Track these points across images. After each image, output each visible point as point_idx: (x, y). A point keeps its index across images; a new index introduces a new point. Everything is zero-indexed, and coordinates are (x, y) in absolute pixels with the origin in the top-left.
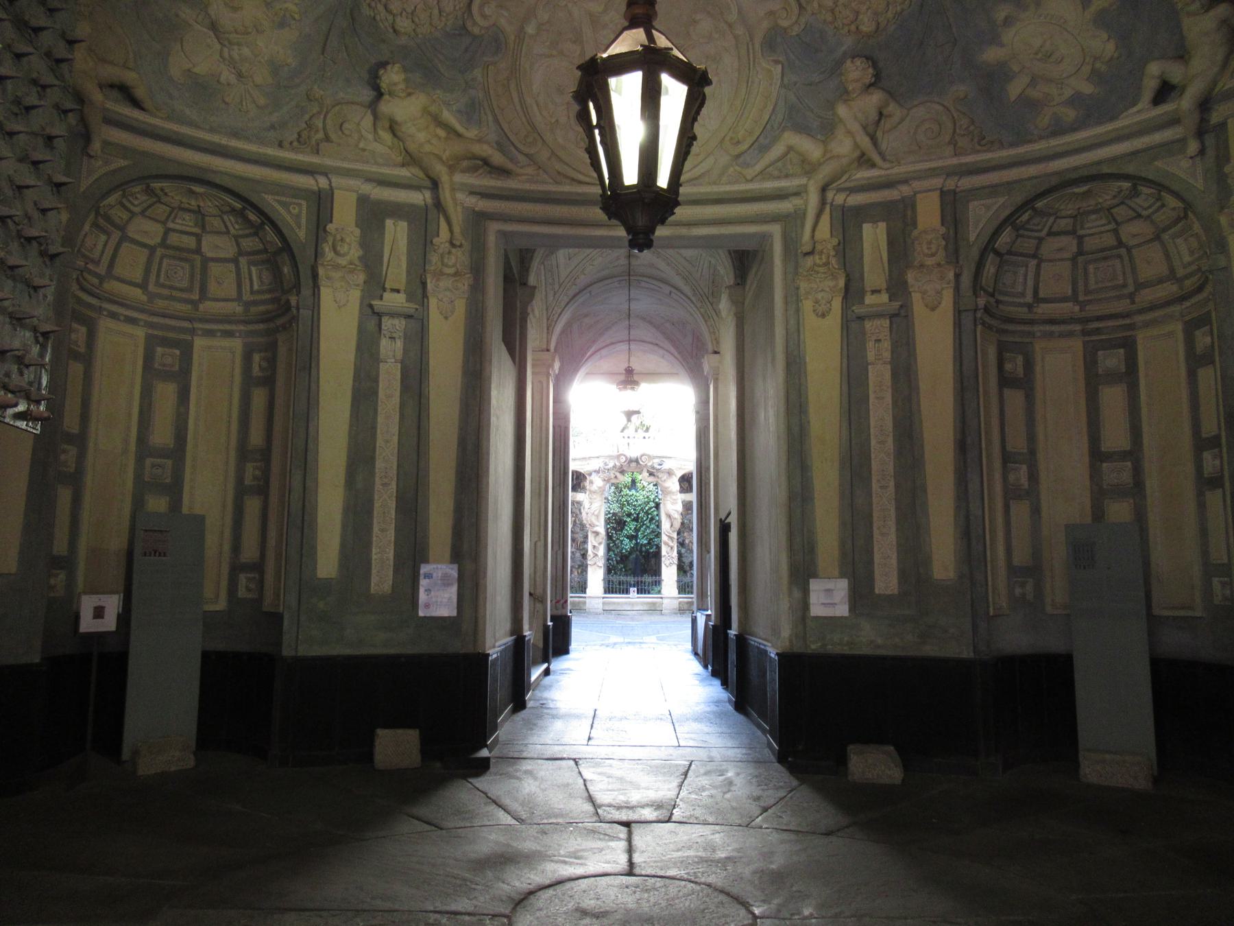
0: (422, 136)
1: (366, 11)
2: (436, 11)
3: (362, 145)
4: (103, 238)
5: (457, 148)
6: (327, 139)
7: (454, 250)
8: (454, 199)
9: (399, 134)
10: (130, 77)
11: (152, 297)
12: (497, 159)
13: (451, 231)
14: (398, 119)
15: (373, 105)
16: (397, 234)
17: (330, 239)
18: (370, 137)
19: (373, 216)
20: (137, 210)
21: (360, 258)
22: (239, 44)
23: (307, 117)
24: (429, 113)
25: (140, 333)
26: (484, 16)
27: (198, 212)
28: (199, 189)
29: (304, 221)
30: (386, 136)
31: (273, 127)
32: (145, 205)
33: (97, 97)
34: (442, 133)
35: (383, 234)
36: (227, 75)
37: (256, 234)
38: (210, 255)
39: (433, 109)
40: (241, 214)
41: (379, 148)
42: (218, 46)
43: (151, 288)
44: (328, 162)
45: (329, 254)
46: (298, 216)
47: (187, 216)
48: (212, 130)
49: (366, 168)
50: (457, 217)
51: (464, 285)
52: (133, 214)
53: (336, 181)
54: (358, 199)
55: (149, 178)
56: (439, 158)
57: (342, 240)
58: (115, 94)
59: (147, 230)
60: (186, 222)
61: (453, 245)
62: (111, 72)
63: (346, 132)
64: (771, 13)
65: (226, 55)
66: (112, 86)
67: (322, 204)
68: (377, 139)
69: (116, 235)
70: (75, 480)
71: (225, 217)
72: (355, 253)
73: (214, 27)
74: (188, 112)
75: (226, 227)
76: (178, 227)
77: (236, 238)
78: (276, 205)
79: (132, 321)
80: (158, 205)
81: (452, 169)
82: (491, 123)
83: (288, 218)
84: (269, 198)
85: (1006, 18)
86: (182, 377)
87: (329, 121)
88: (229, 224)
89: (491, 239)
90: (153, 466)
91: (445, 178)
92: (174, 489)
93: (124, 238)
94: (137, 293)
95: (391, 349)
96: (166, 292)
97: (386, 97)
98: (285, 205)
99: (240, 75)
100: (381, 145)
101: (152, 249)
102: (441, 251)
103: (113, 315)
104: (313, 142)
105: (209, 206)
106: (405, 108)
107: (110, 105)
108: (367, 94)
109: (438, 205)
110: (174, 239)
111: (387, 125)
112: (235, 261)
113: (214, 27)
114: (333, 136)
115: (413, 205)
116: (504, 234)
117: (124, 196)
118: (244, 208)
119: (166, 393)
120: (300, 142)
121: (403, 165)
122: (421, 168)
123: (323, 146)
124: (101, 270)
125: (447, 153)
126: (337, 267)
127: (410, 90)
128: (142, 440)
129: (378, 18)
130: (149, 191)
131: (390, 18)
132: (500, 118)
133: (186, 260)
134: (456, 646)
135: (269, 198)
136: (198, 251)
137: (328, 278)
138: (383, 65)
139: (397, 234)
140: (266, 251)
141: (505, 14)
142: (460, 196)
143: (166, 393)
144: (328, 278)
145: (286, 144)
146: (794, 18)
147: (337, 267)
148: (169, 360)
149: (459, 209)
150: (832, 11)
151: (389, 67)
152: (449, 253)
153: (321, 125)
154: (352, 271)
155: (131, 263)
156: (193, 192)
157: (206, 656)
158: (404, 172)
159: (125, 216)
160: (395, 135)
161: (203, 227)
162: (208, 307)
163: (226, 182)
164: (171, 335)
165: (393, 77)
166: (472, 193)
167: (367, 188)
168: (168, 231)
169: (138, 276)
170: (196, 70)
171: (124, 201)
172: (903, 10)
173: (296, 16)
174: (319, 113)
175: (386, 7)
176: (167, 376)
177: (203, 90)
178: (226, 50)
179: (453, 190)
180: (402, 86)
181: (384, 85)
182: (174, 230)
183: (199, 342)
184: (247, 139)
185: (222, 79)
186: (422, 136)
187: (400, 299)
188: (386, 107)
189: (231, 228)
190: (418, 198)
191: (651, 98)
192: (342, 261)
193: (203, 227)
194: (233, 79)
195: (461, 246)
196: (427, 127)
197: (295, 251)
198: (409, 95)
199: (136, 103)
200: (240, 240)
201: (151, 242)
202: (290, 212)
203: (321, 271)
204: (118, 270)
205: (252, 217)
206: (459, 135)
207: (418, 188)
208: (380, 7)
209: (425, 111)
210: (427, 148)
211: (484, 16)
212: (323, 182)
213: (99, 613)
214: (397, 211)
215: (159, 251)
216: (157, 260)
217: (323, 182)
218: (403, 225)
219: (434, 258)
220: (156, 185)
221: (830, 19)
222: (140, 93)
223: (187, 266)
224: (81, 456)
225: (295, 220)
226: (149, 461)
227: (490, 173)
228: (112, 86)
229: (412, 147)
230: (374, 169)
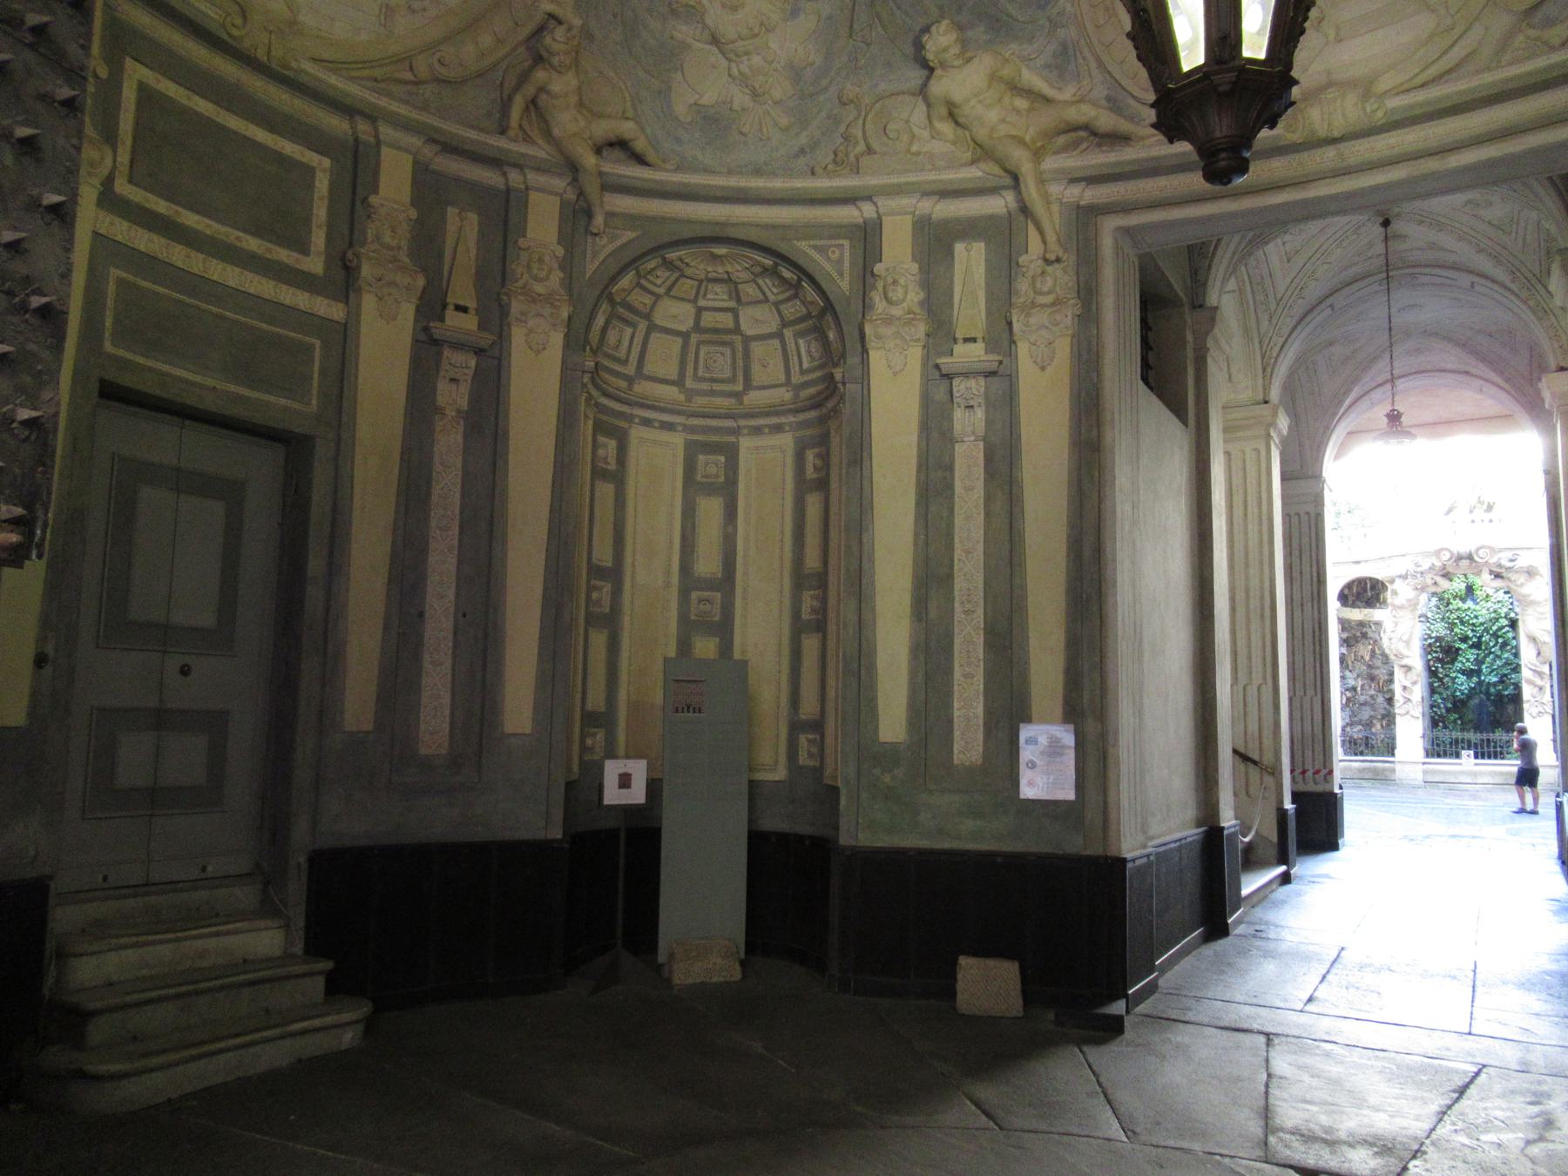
0: (993, 116)
3: (914, 149)
4: (629, 331)
5: (1046, 119)
6: (870, 151)
7: (1049, 269)
8: (1047, 199)
9: (962, 120)
10: (627, 129)
11: (691, 394)
12: (1106, 121)
13: (1044, 242)
14: (957, 97)
15: (923, 91)
16: (971, 261)
17: (880, 285)
18: (925, 134)
19: (936, 242)
20: (661, 291)
21: (921, 304)
22: (746, 53)
23: (842, 129)
24: (1001, 79)
25: (678, 440)
27: (728, 280)
28: (721, 250)
29: (847, 264)
30: (946, 128)
31: (802, 151)
32: (669, 283)
33: (589, 160)
34: (1022, 103)
35: (952, 265)
36: (740, 98)
37: (796, 296)
38: (750, 333)
39: (1006, 72)
40: (773, 272)
41: (937, 147)
42: (725, 63)
43: (689, 383)
44: (874, 181)
45: (880, 305)
46: (840, 261)
47: (718, 288)
48: (730, 172)
49: (912, 178)
50: (1053, 220)
51: (1067, 317)
52: (658, 297)
53: (885, 204)
54: (914, 224)
55: (661, 248)
56: (1021, 141)
57: (895, 282)
58: (617, 153)
59: (674, 313)
60: (718, 296)
61: (1047, 262)
62: (603, 129)
63: (892, 135)
65: (735, 71)
66: (611, 145)
67: (868, 238)
68: (936, 135)
69: (643, 326)
70: (610, 621)
71: (760, 281)
72: (915, 296)
73: (715, 40)
74: (699, 155)
76: (711, 304)
77: (777, 304)
78: (812, 253)
79: (669, 427)
80: (683, 280)
81: (1038, 155)
82: (1095, 72)
83: (828, 267)
84: (803, 245)
86: (728, 490)
87: (869, 126)
89: (1107, 243)
90: (700, 601)
91: (1026, 168)
92: (724, 628)
93: (652, 328)
94: (671, 393)
95: (969, 423)
96: (705, 386)
97: (938, 72)
99: (755, 95)
100: (941, 142)
101: (685, 336)
102: (1031, 273)
103: (647, 422)
104: (852, 159)
105: (738, 270)
106: (965, 82)
107: (607, 168)
108: (915, 76)
109: (1025, 210)
110: (708, 319)
111: (944, 111)
112: (779, 335)
113: (715, 40)
114: (875, 145)
115: (991, 217)
116: (1127, 231)
117: (638, 275)
118: (776, 264)
119: (711, 509)
120: (839, 162)
121: (973, 162)
122: (999, 162)
123: (864, 161)
124: (630, 370)
125: (1032, 131)
126: (889, 320)
127: (969, 54)
128: (686, 569)
130: (668, 265)
132: (1105, 59)
133: (724, 344)
134: (1074, 845)
135: (803, 245)
136: (737, 330)
137: (879, 337)
138: (926, 29)
139: (971, 261)
140: (809, 316)
142: (1055, 189)
143: (711, 509)
144: (879, 337)
145: (819, 170)
147: (889, 320)
148: (712, 470)
149: (1055, 208)
151: (933, 29)
152: (1043, 273)
153: (860, 134)
154: (910, 322)
155: (663, 357)
156: (714, 257)
157: (758, 841)
158: (974, 173)
159: (648, 300)
160: (957, 123)
161: (739, 300)
162: (755, 398)
163: (753, 235)
164: (715, 438)
165: (941, 40)
166: (1074, 181)
167: (926, 206)
168: (700, 310)
169: (672, 371)
170: (704, 101)
171: (643, 282)
174: (857, 119)
176: (710, 489)
177: (715, 124)
178: (733, 65)
179: (1041, 181)
180: (955, 50)
181: (930, 56)
182: (708, 309)
183: (746, 443)
184: (774, 174)
185: (736, 106)
186: (993, 116)
187: (977, 349)
188: (938, 87)
189: (768, 293)
190: (998, 205)
192: (896, 311)
193: (739, 300)
194: (747, 101)
195: (1058, 260)
196: (1000, 100)
197: (837, 308)
198: (969, 60)
199: (640, 160)
200: (782, 307)
201: (683, 328)
202: (829, 259)
203: (868, 330)
204: (649, 368)
205: (787, 274)
206: (1048, 100)
207: (993, 191)
209: (993, 78)
210: (1003, 130)
212: (868, 210)
213: (625, 781)
214: (969, 229)
215: (694, 338)
216: (692, 350)
217: (868, 210)
218: (979, 248)
219: (1023, 286)
220: (673, 255)
222: (640, 145)
223: (728, 351)
224: (617, 592)
225: (834, 266)
226: (694, 595)
227: (1099, 145)
228: (611, 145)
229: (982, 134)
230: (932, 176)
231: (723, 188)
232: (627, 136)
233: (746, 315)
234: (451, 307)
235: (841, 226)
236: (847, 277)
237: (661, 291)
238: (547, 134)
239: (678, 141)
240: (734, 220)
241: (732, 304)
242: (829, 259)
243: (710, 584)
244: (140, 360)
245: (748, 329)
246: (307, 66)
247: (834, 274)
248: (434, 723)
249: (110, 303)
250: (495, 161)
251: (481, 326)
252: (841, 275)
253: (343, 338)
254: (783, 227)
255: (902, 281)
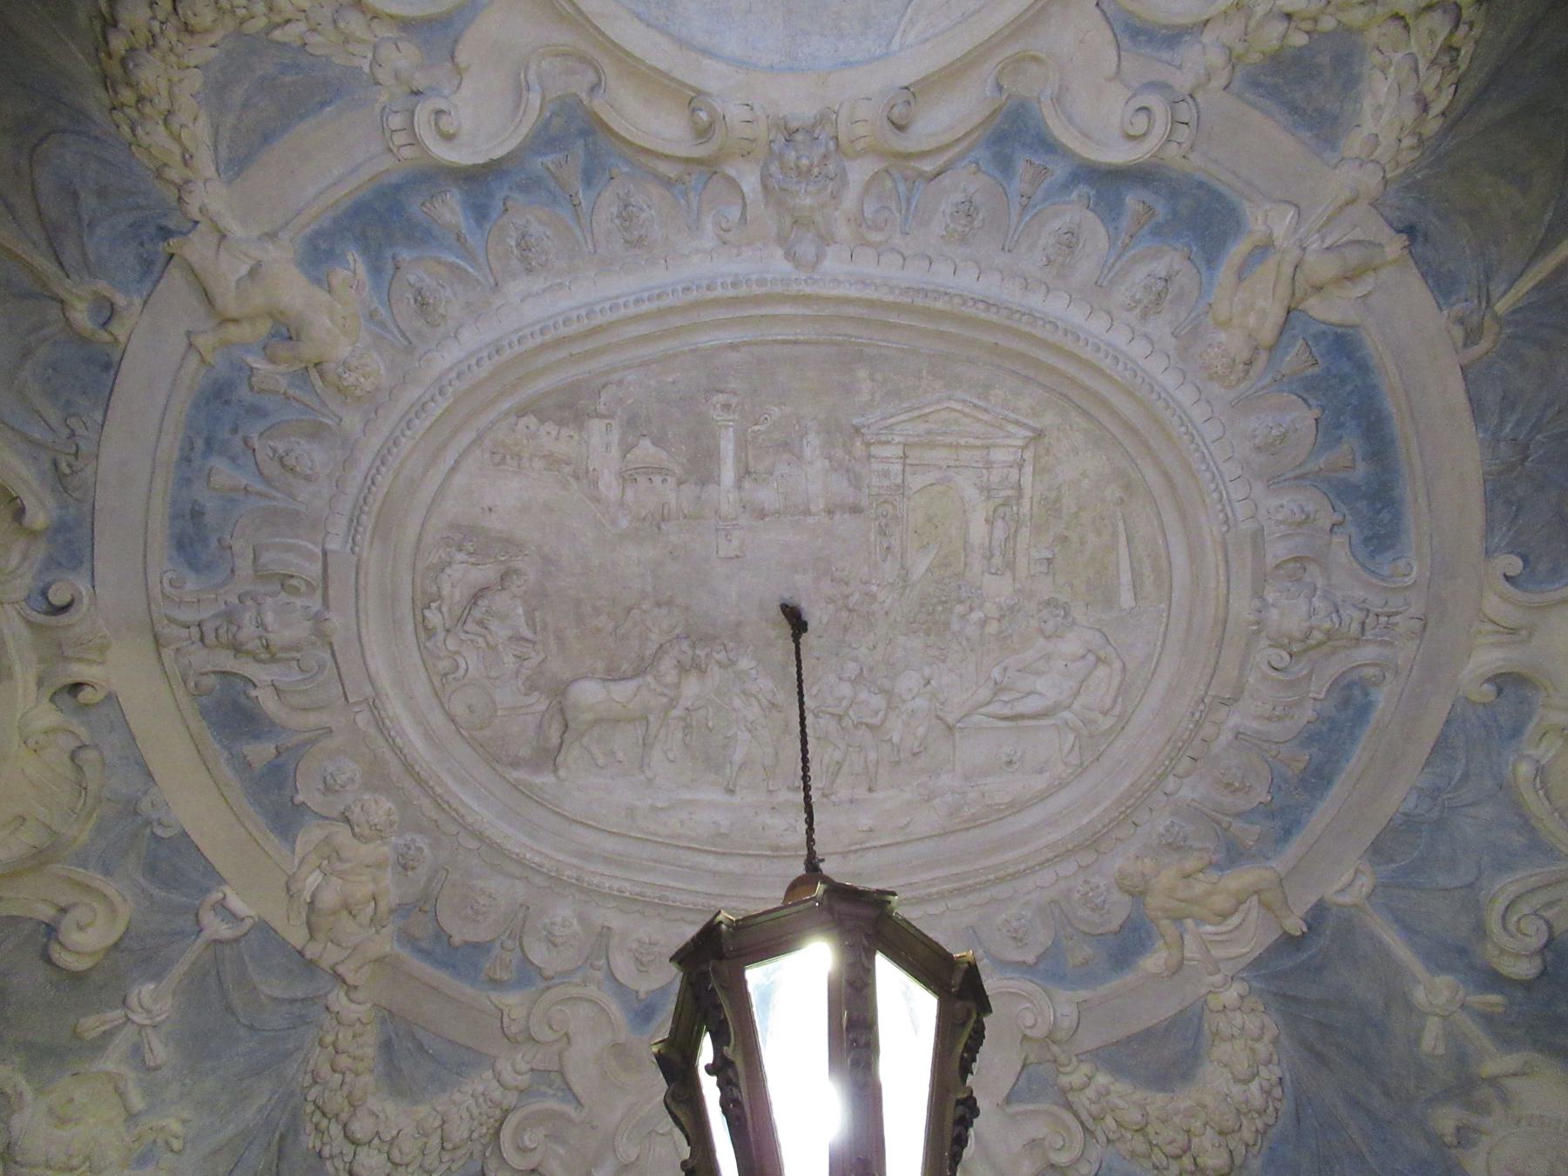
1: (310, 1141)
2: (435, 1141)
26: (522, 1150)
64: (1034, 1144)
85: (1458, 1129)
129: (326, 1153)
131: (348, 1149)
141: (561, 1151)
146: (1077, 1151)
150: (1141, 1131)
172: (1268, 1126)
173: (176, 1145)
175: (345, 1126)
191: (854, 1032)
208: (335, 1129)
211: (522, 1150)
221: (1141, 1148)
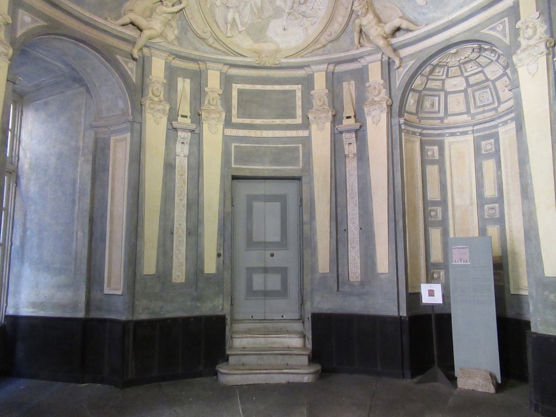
4: (437, 98)
11: (473, 116)
20: (444, 77)
25: (470, 138)
28: (453, 51)
32: (445, 73)
38: (493, 78)
43: (473, 111)
47: (470, 65)
59: (455, 83)
69: (442, 94)
70: (443, 224)
75: (489, 59)
78: (492, 33)
79: (465, 133)
84: (485, 31)
86: (496, 155)
88: (489, 56)
90: (489, 209)
92: (501, 221)
93: (447, 94)
94: (465, 117)
96: (481, 110)
98: (493, 29)
103: (453, 134)
110: (472, 80)
119: (489, 165)
124: (442, 114)
133: (485, 88)
135: (485, 31)
136: (487, 80)
137: (520, 60)
143: (489, 165)
144: (520, 60)
148: (489, 147)
155: (456, 103)
159: (439, 83)
161: (481, 66)
164: (487, 132)
168: (466, 78)
169: (462, 108)
176: (488, 156)
189: (492, 58)
193: (481, 66)
199: (408, 30)
204: (450, 112)
213: (431, 293)
216: (471, 96)
224: (445, 211)
226: (486, 207)
231: (443, 24)
232: (397, 25)
233: (487, 71)
234: (345, 118)
235: (502, 12)
236: (508, 36)
237: (444, 77)
238: (370, 41)
239: (424, 14)
240: (453, 35)
241: (480, 69)
242: (498, 31)
243: (492, 201)
244: (244, 167)
245: (491, 77)
246: (283, 60)
247: (501, 37)
248: (179, 274)
249: (233, 153)
250: (354, 60)
251: (356, 121)
252: (505, 36)
253: (307, 142)
254: (476, 26)
255: (531, 25)
